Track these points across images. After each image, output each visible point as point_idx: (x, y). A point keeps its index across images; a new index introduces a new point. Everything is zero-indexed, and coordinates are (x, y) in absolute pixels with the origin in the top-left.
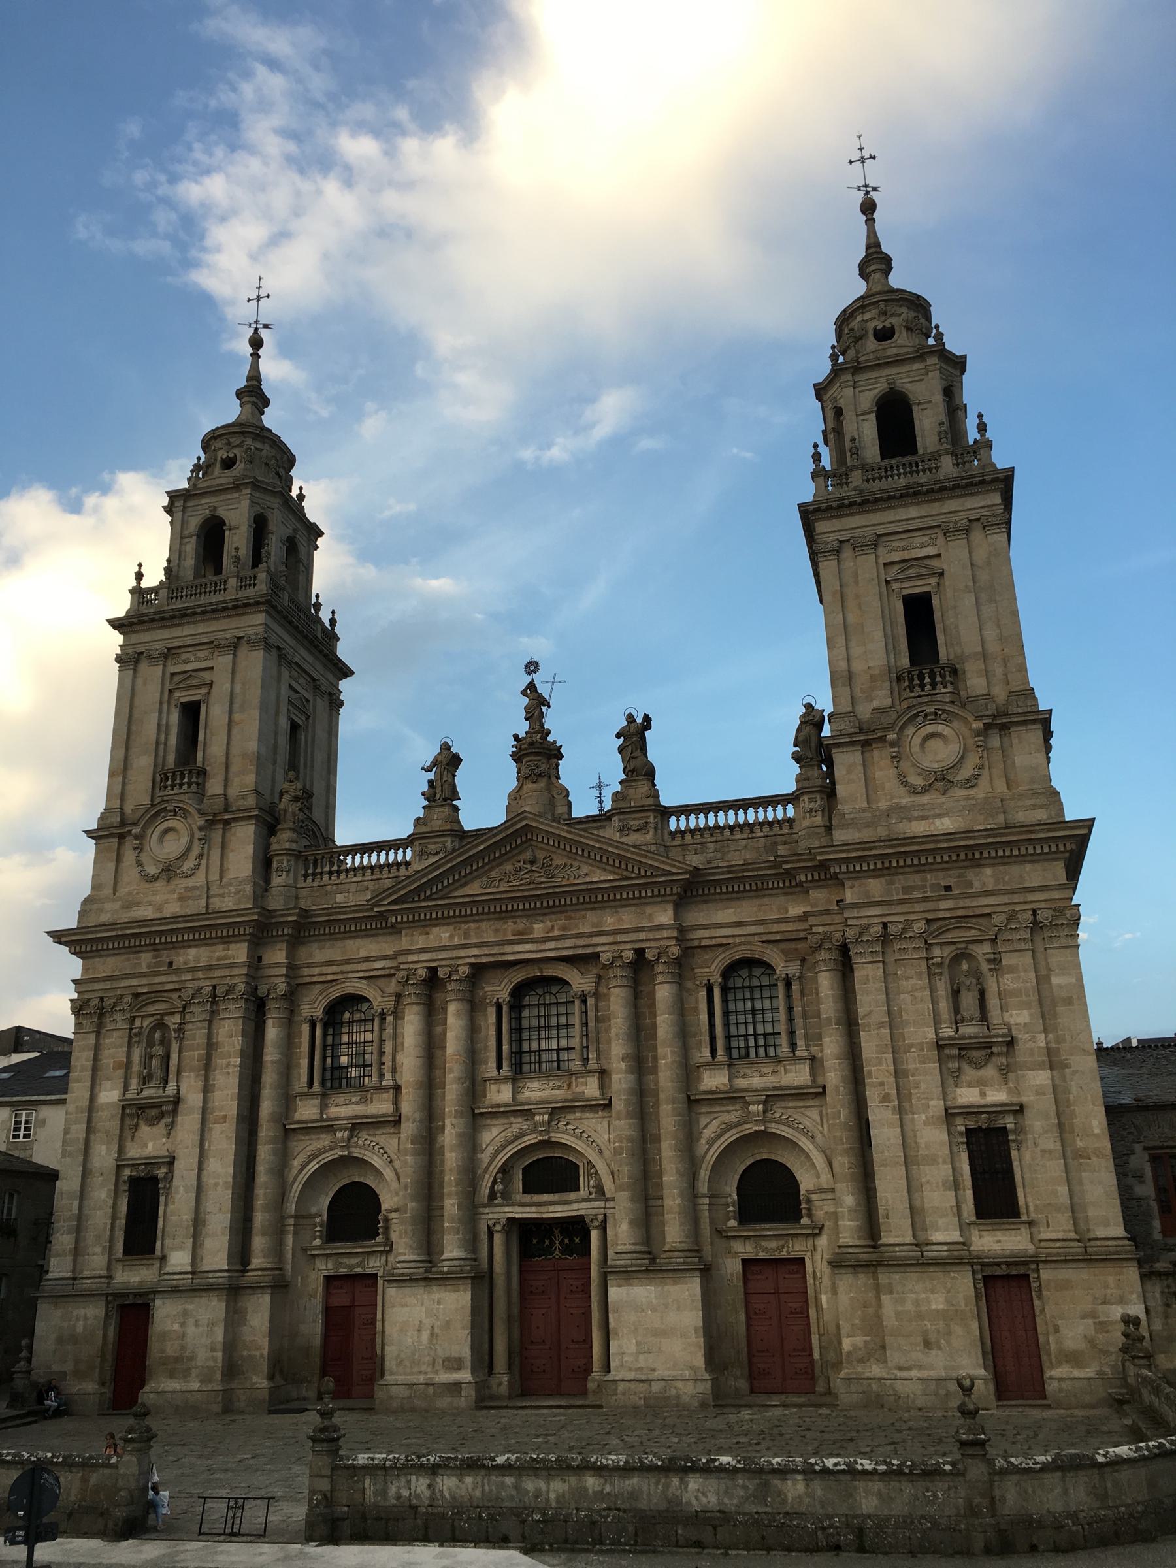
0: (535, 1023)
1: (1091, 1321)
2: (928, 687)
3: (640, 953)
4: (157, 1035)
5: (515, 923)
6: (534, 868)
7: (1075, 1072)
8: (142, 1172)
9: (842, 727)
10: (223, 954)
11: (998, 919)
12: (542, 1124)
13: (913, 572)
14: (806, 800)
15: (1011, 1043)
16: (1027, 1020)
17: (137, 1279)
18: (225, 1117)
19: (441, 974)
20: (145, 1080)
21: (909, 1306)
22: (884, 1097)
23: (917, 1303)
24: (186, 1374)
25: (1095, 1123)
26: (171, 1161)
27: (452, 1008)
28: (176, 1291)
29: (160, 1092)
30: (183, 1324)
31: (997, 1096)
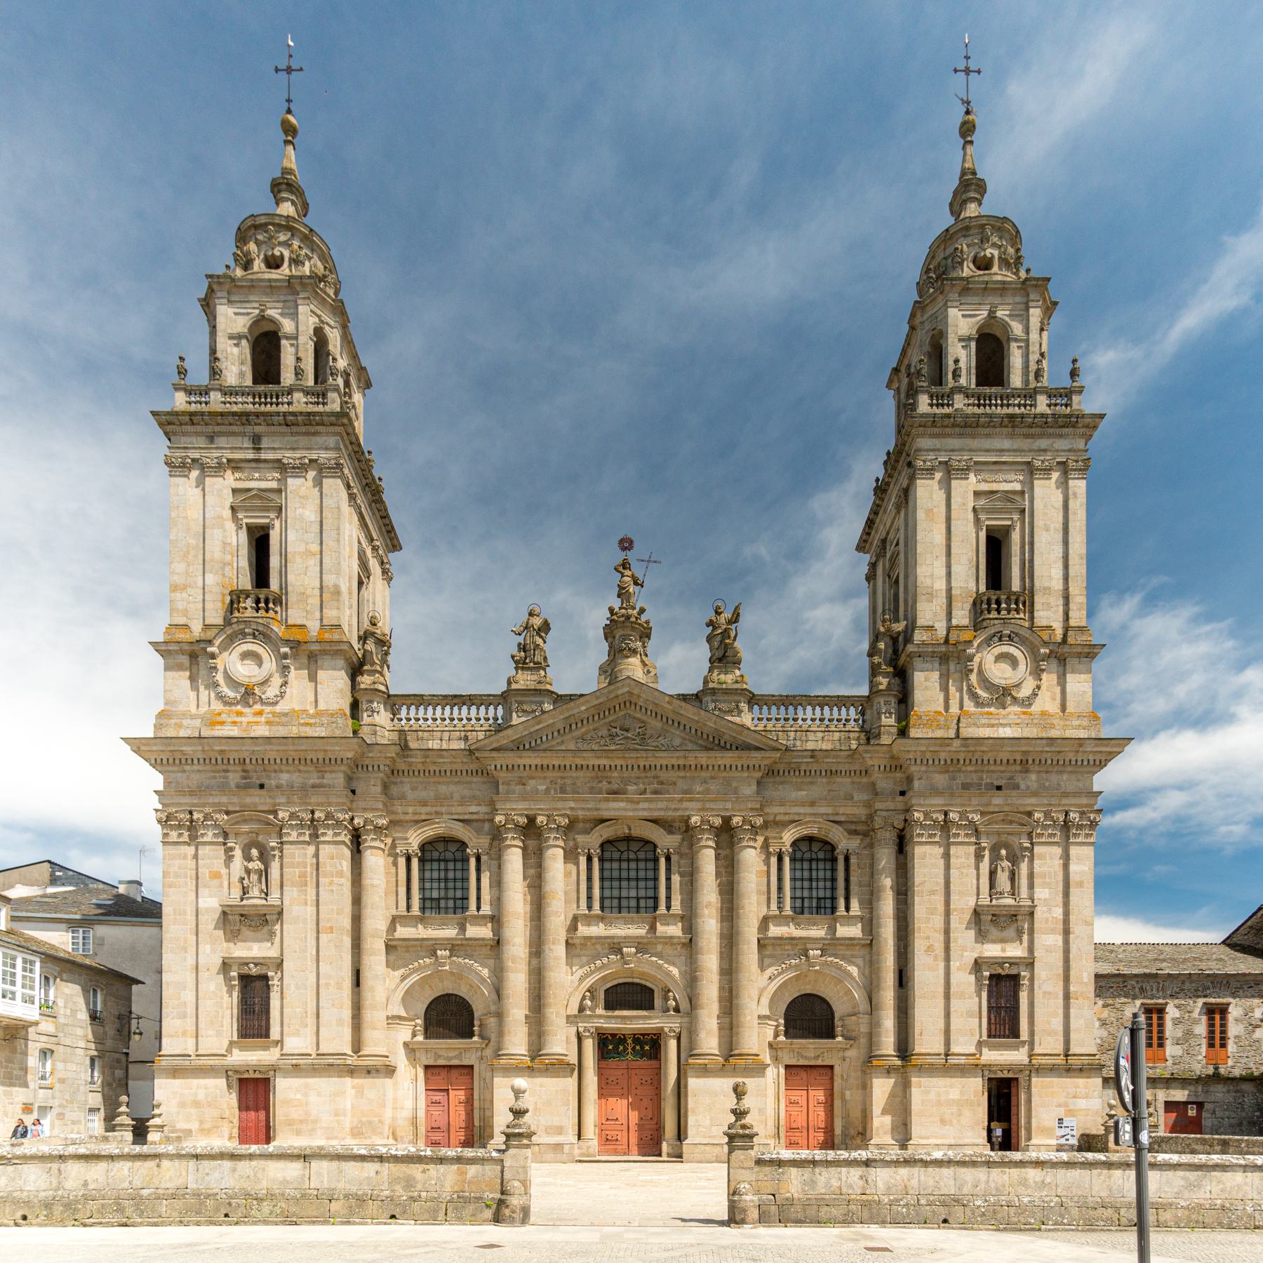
0: (616, 874)
1: (1063, 1109)
2: (1003, 612)
3: (726, 820)
4: (255, 852)
5: (610, 783)
7: (1077, 937)
8: (254, 971)
9: (924, 638)
10: (318, 781)
11: (1037, 815)
12: (629, 955)
13: (999, 504)
15: (1032, 914)
16: (1047, 896)
17: (255, 1058)
18: (331, 928)
19: (541, 820)
20: (245, 891)
21: (932, 1096)
22: (929, 947)
23: (939, 1094)
24: (312, 1132)
25: (1085, 975)
26: (279, 965)
27: (550, 853)
28: (296, 1070)
29: (264, 902)
30: (306, 1095)
31: (1016, 951)
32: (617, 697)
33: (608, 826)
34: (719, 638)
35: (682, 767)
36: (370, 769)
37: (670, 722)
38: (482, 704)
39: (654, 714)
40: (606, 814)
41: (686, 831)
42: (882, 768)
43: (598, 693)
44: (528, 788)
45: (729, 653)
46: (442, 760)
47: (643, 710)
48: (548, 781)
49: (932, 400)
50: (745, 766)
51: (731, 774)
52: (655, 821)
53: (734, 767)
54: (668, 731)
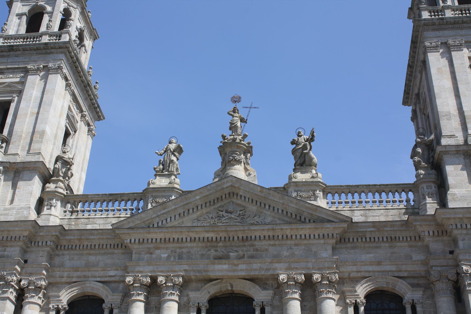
3: (309, 277)
5: (216, 251)
6: (232, 216)
14: (425, 187)
32: (223, 189)
33: (215, 285)
34: (300, 150)
35: (271, 237)
36: (40, 244)
37: (263, 205)
38: (129, 200)
39: (250, 201)
40: (212, 275)
41: (277, 288)
42: (431, 233)
43: (209, 187)
44: (154, 256)
45: (307, 159)
46: (92, 237)
47: (243, 198)
48: (169, 251)
49: (431, 13)
50: (321, 235)
51: (311, 242)
52: (252, 280)
53: (312, 236)
54: (262, 213)
